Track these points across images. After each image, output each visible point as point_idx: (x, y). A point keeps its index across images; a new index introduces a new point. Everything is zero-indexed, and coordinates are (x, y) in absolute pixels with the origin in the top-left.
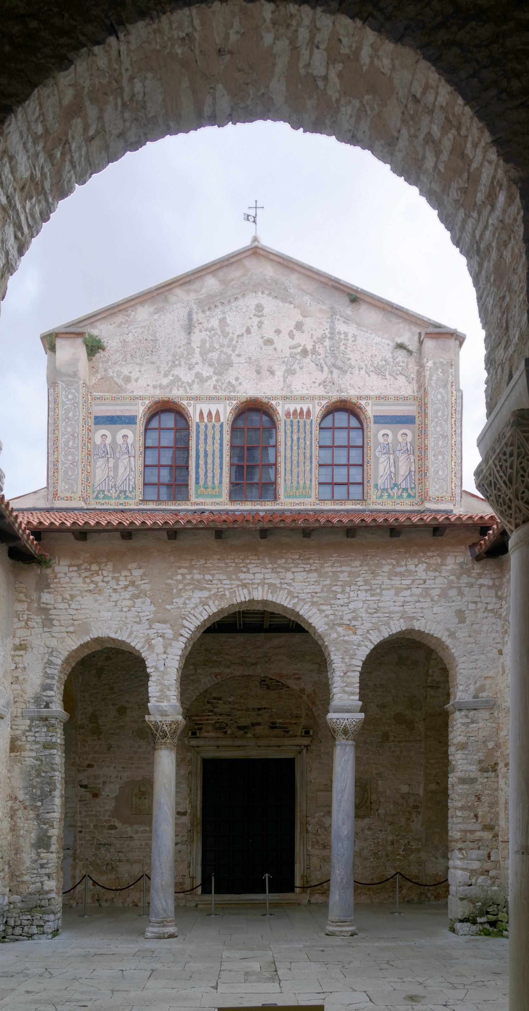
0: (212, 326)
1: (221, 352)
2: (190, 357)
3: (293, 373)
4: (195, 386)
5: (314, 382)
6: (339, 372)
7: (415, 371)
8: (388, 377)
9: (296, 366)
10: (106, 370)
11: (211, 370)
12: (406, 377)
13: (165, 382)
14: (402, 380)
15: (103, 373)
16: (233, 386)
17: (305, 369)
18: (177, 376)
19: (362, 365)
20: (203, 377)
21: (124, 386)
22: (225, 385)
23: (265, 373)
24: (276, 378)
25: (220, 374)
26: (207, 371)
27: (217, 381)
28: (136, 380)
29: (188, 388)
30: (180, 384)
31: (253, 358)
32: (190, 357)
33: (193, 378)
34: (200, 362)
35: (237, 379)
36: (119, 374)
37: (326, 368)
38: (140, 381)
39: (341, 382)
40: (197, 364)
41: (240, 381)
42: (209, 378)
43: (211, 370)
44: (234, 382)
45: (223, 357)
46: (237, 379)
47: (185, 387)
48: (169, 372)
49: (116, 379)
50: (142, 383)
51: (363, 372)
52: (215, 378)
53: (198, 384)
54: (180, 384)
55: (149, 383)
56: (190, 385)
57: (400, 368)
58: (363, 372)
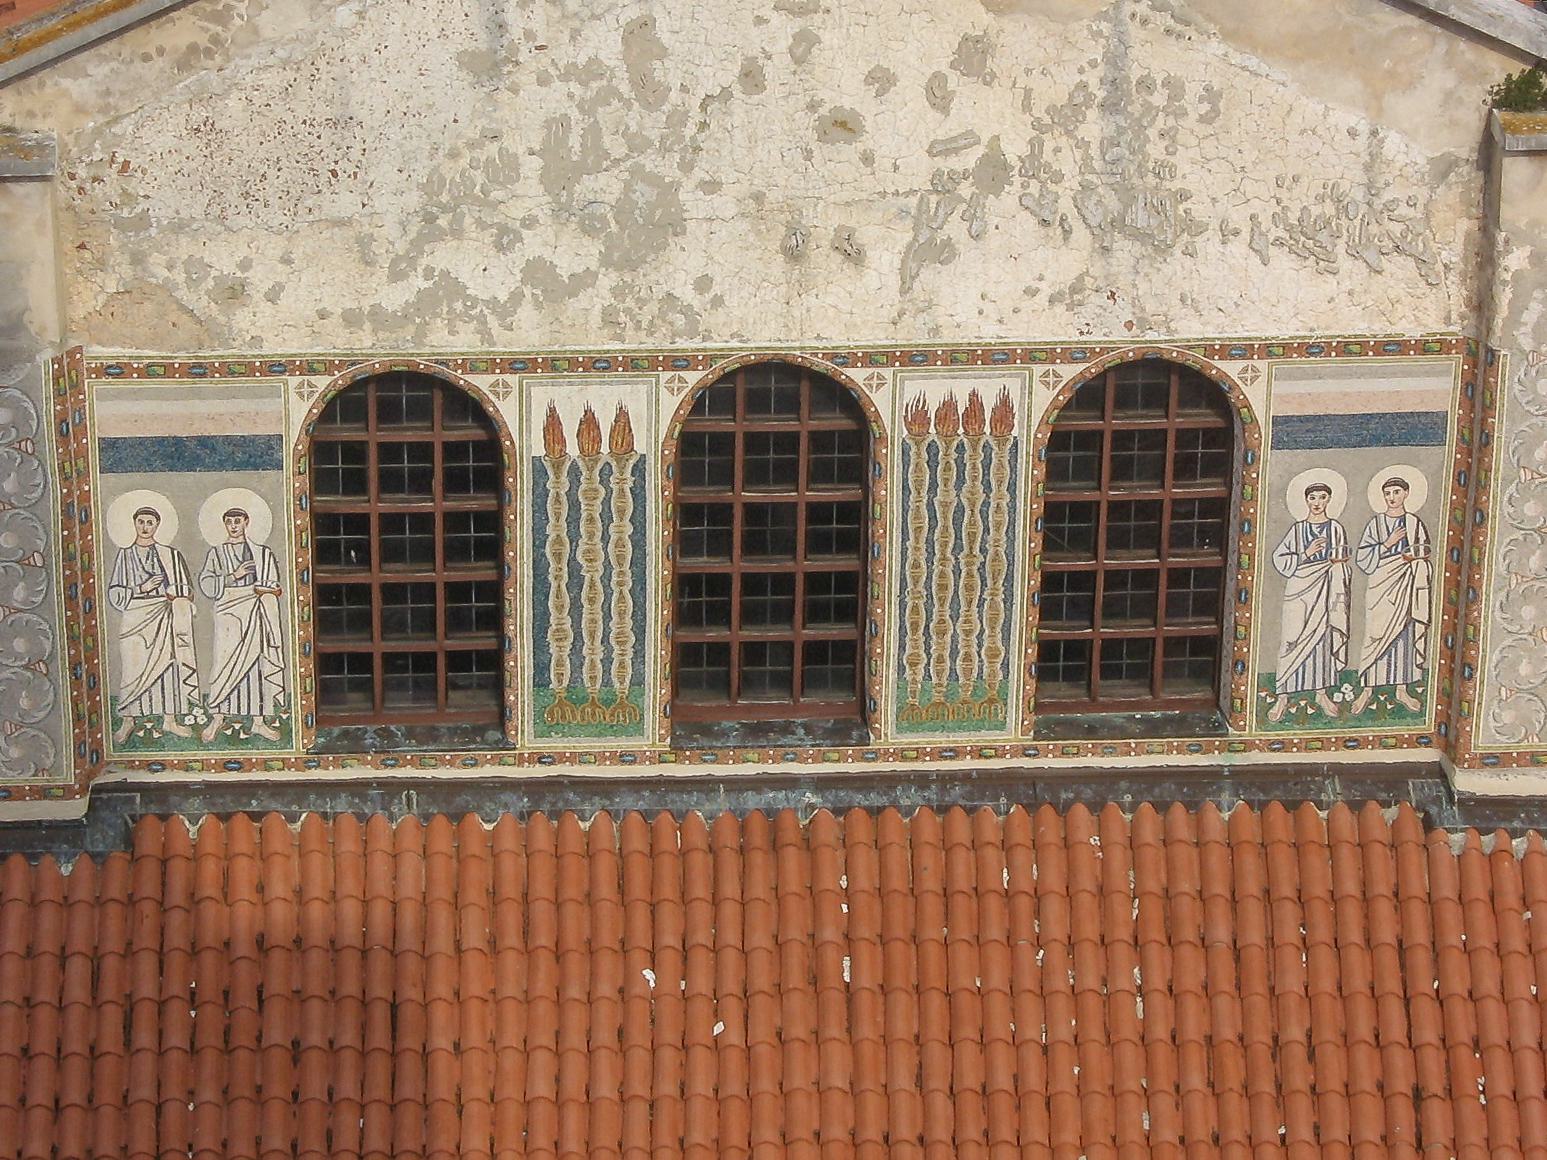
0: (594, 60)
1: (637, 172)
2: (497, 194)
3: (944, 253)
4: (526, 314)
5: (1031, 292)
6: (1137, 248)
7: (1460, 240)
8: (1345, 263)
9: (955, 229)
10: (138, 259)
11: (594, 248)
12: (1420, 261)
13: (395, 297)
14: (1399, 268)
15: (127, 271)
16: (687, 311)
17: (993, 240)
18: (446, 274)
19: (1239, 219)
20: (556, 277)
21: (222, 319)
22: (652, 308)
23: (823, 259)
24: (871, 279)
25: (630, 264)
26: (573, 254)
27: (618, 292)
28: (272, 296)
29: (493, 322)
30: (459, 306)
31: (774, 196)
32: (497, 194)
33: (514, 282)
34: (544, 215)
35: (703, 284)
36: (196, 269)
37: (1081, 234)
38: (285, 299)
39: (1143, 287)
40: (530, 222)
41: (716, 289)
42: (582, 281)
43: (594, 248)
44: (687, 294)
45: (643, 194)
46: (703, 284)
47: (482, 320)
48: (412, 262)
49: (183, 294)
50: (298, 301)
51: (1238, 247)
52: (607, 280)
53: (538, 306)
54: (459, 306)
55: (326, 304)
56: (505, 311)
57: (1397, 229)
58: (1238, 247)
